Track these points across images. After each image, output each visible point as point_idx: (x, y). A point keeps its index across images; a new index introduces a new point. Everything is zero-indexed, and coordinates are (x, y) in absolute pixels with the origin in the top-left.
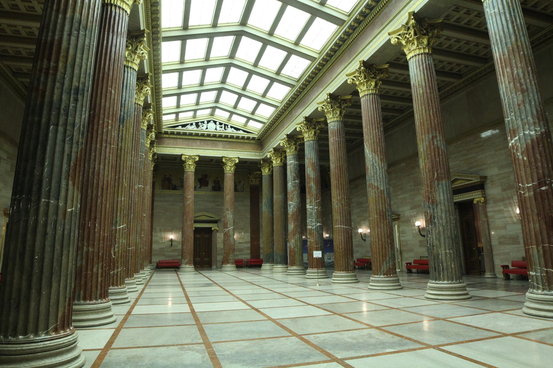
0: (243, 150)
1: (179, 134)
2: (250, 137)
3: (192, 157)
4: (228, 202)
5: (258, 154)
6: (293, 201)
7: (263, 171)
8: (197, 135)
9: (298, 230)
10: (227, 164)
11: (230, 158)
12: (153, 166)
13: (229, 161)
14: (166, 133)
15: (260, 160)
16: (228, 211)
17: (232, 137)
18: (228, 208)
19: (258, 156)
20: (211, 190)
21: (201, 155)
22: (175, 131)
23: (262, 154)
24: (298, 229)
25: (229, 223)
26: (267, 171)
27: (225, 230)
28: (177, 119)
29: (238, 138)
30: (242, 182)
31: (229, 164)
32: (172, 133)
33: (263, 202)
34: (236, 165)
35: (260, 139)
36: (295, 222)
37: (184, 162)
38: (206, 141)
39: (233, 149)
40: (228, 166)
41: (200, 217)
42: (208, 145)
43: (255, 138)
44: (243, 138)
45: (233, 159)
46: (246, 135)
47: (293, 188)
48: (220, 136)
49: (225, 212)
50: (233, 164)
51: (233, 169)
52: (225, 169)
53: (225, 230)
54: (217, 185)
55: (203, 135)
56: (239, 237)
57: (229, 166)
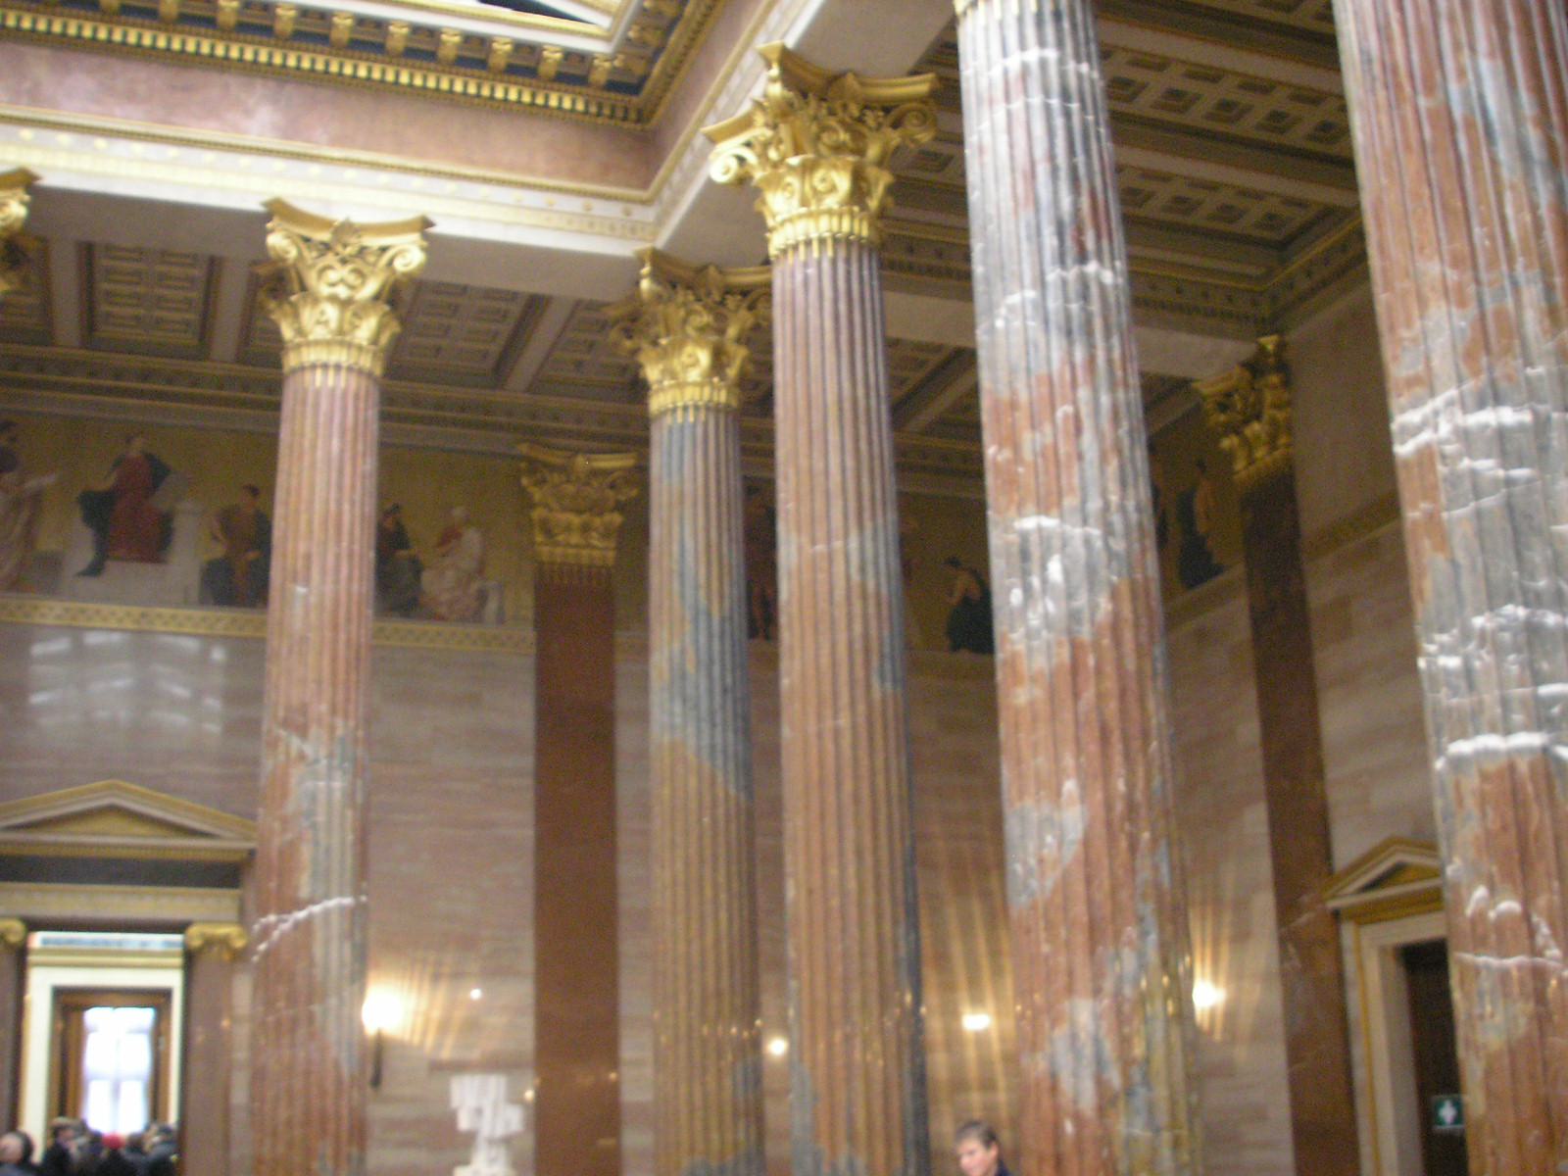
0: (472, 163)
2: (533, 50)
4: (304, 640)
5: (614, 210)
6: (1070, 501)
9: (1145, 874)
10: (311, 278)
11: (346, 230)
13: (330, 259)
15: (628, 269)
16: (302, 731)
18: (304, 709)
19: (612, 230)
20: (194, 593)
21: (50, 180)
23: (648, 214)
24: (1144, 864)
25: (306, 852)
26: (694, 375)
27: (266, 932)
30: (472, 538)
31: (331, 280)
33: (660, 662)
34: (397, 296)
35: (639, 68)
36: (1106, 775)
38: (116, 65)
39: (379, 149)
40: (316, 300)
41: (75, 827)
42: (131, 97)
43: (583, 58)
45: (373, 242)
47: (1057, 343)
49: (274, 744)
50: (371, 287)
51: (366, 330)
52: (287, 332)
53: (266, 932)
54: (252, 556)
56: (436, 1014)
57: (333, 299)
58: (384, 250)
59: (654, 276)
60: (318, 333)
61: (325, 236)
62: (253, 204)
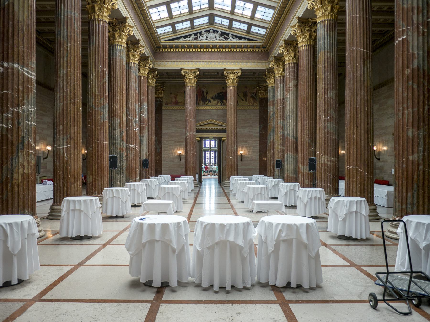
1: (177, 47)
3: (192, 71)
7: (268, 82)
8: (196, 47)
10: (229, 77)
12: (154, 82)
14: (165, 47)
17: (233, 47)
21: (201, 68)
22: (173, 44)
28: (174, 31)
29: (239, 47)
31: (232, 77)
32: (171, 47)
35: (265, 46)
37: (184, 77)
44: (245, 47)
45: (235, 71)
46: (249, 44)
48: (221, 47)
55: (202, 47)
57: (231, 79)
58: (237, 72)
59: (267, 72)
60: (231, 83)
61: (230, 71)
62: (222, 68)
